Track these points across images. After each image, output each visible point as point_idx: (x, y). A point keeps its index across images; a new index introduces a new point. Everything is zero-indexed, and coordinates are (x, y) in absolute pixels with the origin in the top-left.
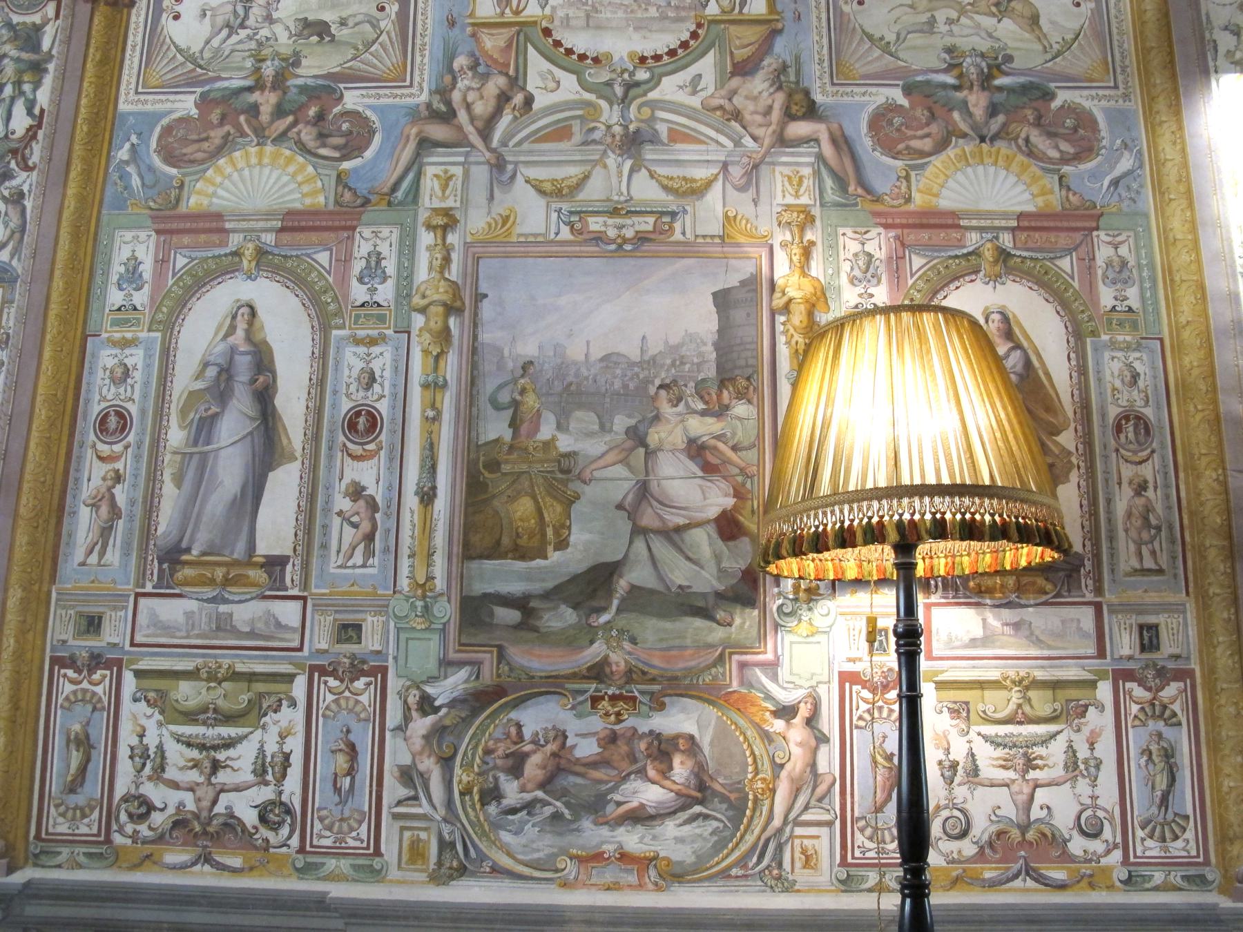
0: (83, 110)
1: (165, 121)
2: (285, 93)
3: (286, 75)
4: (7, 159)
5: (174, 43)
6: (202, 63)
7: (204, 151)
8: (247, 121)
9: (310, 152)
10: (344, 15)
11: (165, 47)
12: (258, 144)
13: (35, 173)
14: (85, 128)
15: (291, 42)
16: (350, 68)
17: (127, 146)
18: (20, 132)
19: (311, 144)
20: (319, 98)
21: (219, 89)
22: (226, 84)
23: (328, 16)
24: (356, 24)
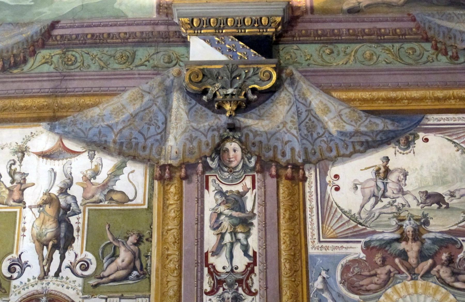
0: (283, 253)
1: (343, 262)
2: (423, 243)
3: (421, 230)
4: (236, 287)
5: (339, 207)
6: (361, 221)
7: (376, 284)
8: (400, 262)
9: (449, 285)
10: (452, 189)
11: (333, 210)
12: (412, 279)
13: (258, 297)
14: (287, 266)
15: (419, 207)
16: (462, 226)
17: (320, 279)
18: (242, 268)
19: (449, 280)
20: (447, 247)
21: (377, 240)
22: (380, 236)
23: (441, 190)
24: (462, 196)
